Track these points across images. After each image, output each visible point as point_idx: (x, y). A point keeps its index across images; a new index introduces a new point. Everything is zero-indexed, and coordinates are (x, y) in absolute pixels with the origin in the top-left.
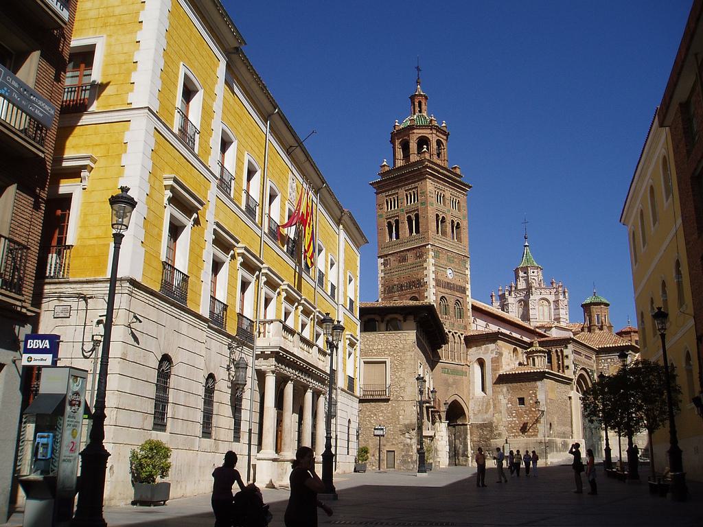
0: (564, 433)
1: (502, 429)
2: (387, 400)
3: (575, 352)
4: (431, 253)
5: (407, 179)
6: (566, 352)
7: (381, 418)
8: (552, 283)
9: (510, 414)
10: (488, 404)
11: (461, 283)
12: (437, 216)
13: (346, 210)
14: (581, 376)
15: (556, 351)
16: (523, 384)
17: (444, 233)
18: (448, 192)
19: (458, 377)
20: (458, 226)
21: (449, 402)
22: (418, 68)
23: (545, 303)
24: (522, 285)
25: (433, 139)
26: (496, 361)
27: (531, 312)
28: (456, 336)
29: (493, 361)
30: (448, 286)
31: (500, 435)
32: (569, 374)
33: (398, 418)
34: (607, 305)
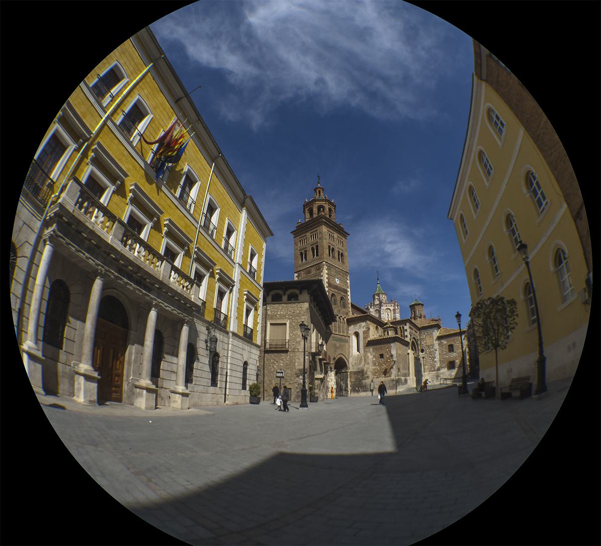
0: (405, 374)
1: (369, 374)
2: (287, 351)
3: (410, 328)
4: (325, 267)
5: (311, 227)
6: (406, 327)
7: (282, 364)
8: (392, 301)
9: (374, 364)
10: (361, 359)
11: (344, 287)
12: (329, 246)
13: (248, 195)
14: (413, 342)
15: (400, 328)
16: (383, 345)
17: (333, 257)
18: (336, 235)
19: (342, 343)
20: (342, 255)
21: (337, 359)
22: (318, 176)
23: (389, 311)
24: (377, 302)
25: (327, 207)
26: (366, 333)
27: (382, 315)
28: (342, 318)
29: (364, 333)
30: (336, 287)
31: (368, 377)
32: (408, 339)
33: (294, 364)
34: (422, 305)
